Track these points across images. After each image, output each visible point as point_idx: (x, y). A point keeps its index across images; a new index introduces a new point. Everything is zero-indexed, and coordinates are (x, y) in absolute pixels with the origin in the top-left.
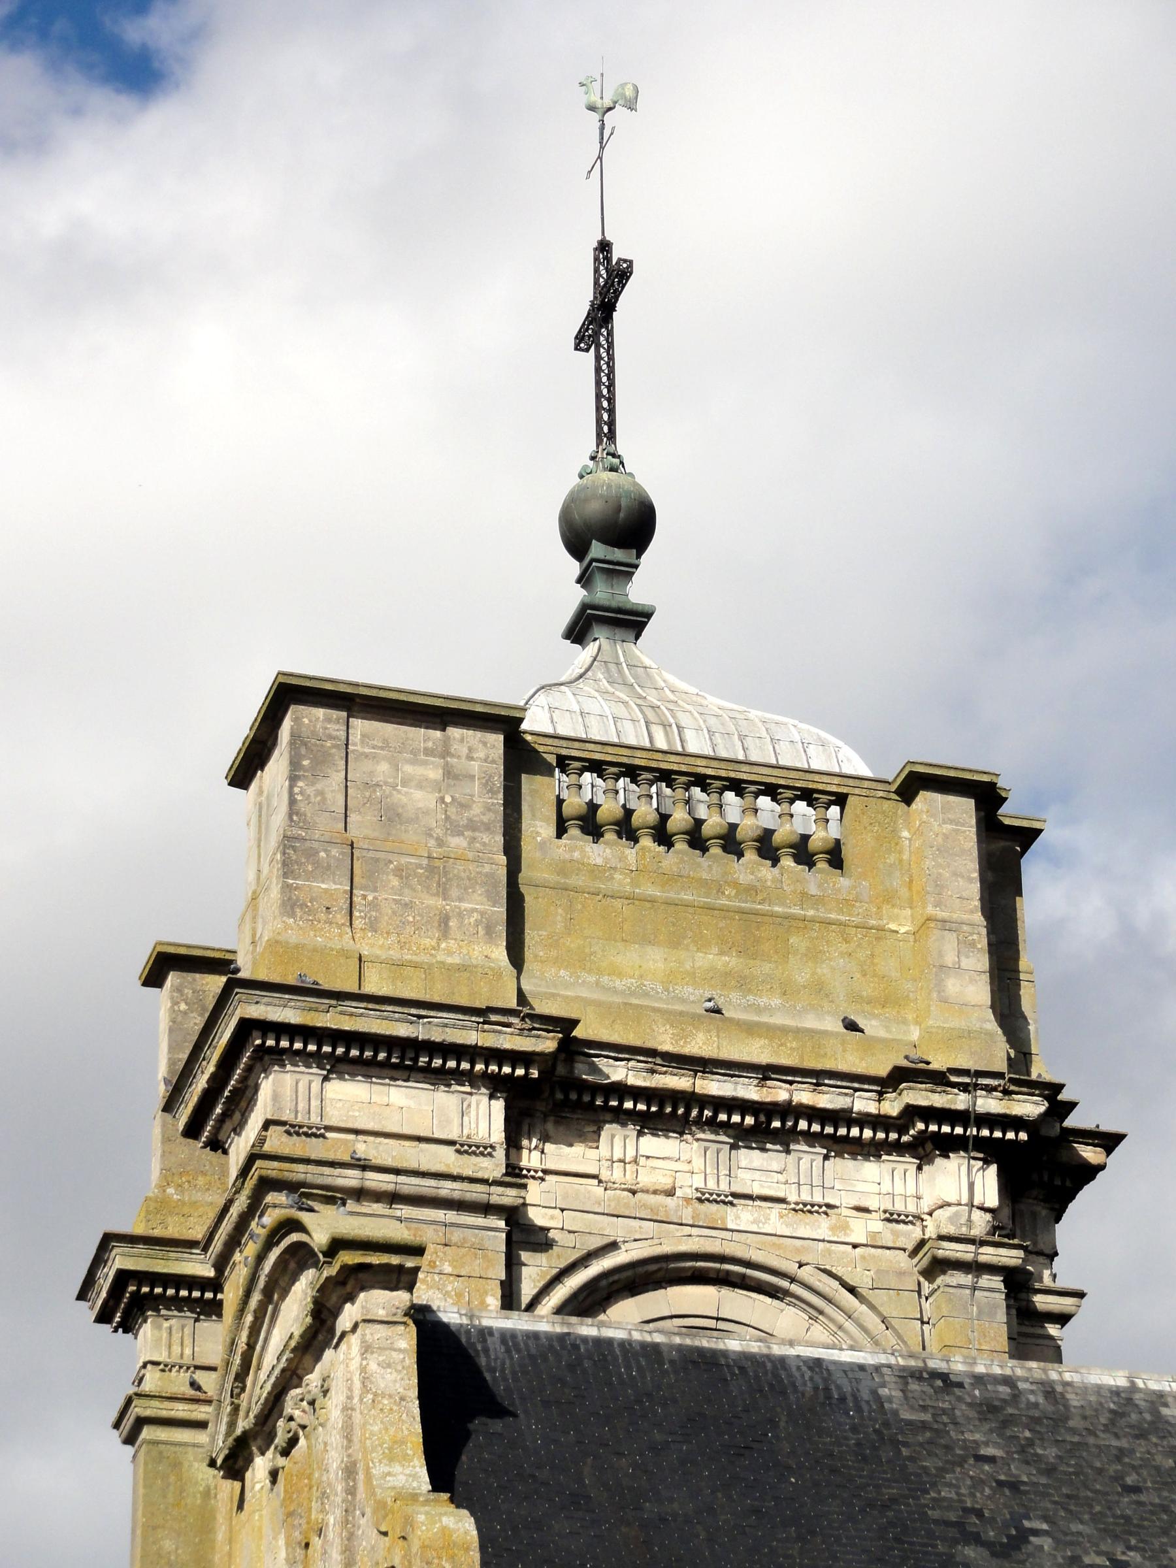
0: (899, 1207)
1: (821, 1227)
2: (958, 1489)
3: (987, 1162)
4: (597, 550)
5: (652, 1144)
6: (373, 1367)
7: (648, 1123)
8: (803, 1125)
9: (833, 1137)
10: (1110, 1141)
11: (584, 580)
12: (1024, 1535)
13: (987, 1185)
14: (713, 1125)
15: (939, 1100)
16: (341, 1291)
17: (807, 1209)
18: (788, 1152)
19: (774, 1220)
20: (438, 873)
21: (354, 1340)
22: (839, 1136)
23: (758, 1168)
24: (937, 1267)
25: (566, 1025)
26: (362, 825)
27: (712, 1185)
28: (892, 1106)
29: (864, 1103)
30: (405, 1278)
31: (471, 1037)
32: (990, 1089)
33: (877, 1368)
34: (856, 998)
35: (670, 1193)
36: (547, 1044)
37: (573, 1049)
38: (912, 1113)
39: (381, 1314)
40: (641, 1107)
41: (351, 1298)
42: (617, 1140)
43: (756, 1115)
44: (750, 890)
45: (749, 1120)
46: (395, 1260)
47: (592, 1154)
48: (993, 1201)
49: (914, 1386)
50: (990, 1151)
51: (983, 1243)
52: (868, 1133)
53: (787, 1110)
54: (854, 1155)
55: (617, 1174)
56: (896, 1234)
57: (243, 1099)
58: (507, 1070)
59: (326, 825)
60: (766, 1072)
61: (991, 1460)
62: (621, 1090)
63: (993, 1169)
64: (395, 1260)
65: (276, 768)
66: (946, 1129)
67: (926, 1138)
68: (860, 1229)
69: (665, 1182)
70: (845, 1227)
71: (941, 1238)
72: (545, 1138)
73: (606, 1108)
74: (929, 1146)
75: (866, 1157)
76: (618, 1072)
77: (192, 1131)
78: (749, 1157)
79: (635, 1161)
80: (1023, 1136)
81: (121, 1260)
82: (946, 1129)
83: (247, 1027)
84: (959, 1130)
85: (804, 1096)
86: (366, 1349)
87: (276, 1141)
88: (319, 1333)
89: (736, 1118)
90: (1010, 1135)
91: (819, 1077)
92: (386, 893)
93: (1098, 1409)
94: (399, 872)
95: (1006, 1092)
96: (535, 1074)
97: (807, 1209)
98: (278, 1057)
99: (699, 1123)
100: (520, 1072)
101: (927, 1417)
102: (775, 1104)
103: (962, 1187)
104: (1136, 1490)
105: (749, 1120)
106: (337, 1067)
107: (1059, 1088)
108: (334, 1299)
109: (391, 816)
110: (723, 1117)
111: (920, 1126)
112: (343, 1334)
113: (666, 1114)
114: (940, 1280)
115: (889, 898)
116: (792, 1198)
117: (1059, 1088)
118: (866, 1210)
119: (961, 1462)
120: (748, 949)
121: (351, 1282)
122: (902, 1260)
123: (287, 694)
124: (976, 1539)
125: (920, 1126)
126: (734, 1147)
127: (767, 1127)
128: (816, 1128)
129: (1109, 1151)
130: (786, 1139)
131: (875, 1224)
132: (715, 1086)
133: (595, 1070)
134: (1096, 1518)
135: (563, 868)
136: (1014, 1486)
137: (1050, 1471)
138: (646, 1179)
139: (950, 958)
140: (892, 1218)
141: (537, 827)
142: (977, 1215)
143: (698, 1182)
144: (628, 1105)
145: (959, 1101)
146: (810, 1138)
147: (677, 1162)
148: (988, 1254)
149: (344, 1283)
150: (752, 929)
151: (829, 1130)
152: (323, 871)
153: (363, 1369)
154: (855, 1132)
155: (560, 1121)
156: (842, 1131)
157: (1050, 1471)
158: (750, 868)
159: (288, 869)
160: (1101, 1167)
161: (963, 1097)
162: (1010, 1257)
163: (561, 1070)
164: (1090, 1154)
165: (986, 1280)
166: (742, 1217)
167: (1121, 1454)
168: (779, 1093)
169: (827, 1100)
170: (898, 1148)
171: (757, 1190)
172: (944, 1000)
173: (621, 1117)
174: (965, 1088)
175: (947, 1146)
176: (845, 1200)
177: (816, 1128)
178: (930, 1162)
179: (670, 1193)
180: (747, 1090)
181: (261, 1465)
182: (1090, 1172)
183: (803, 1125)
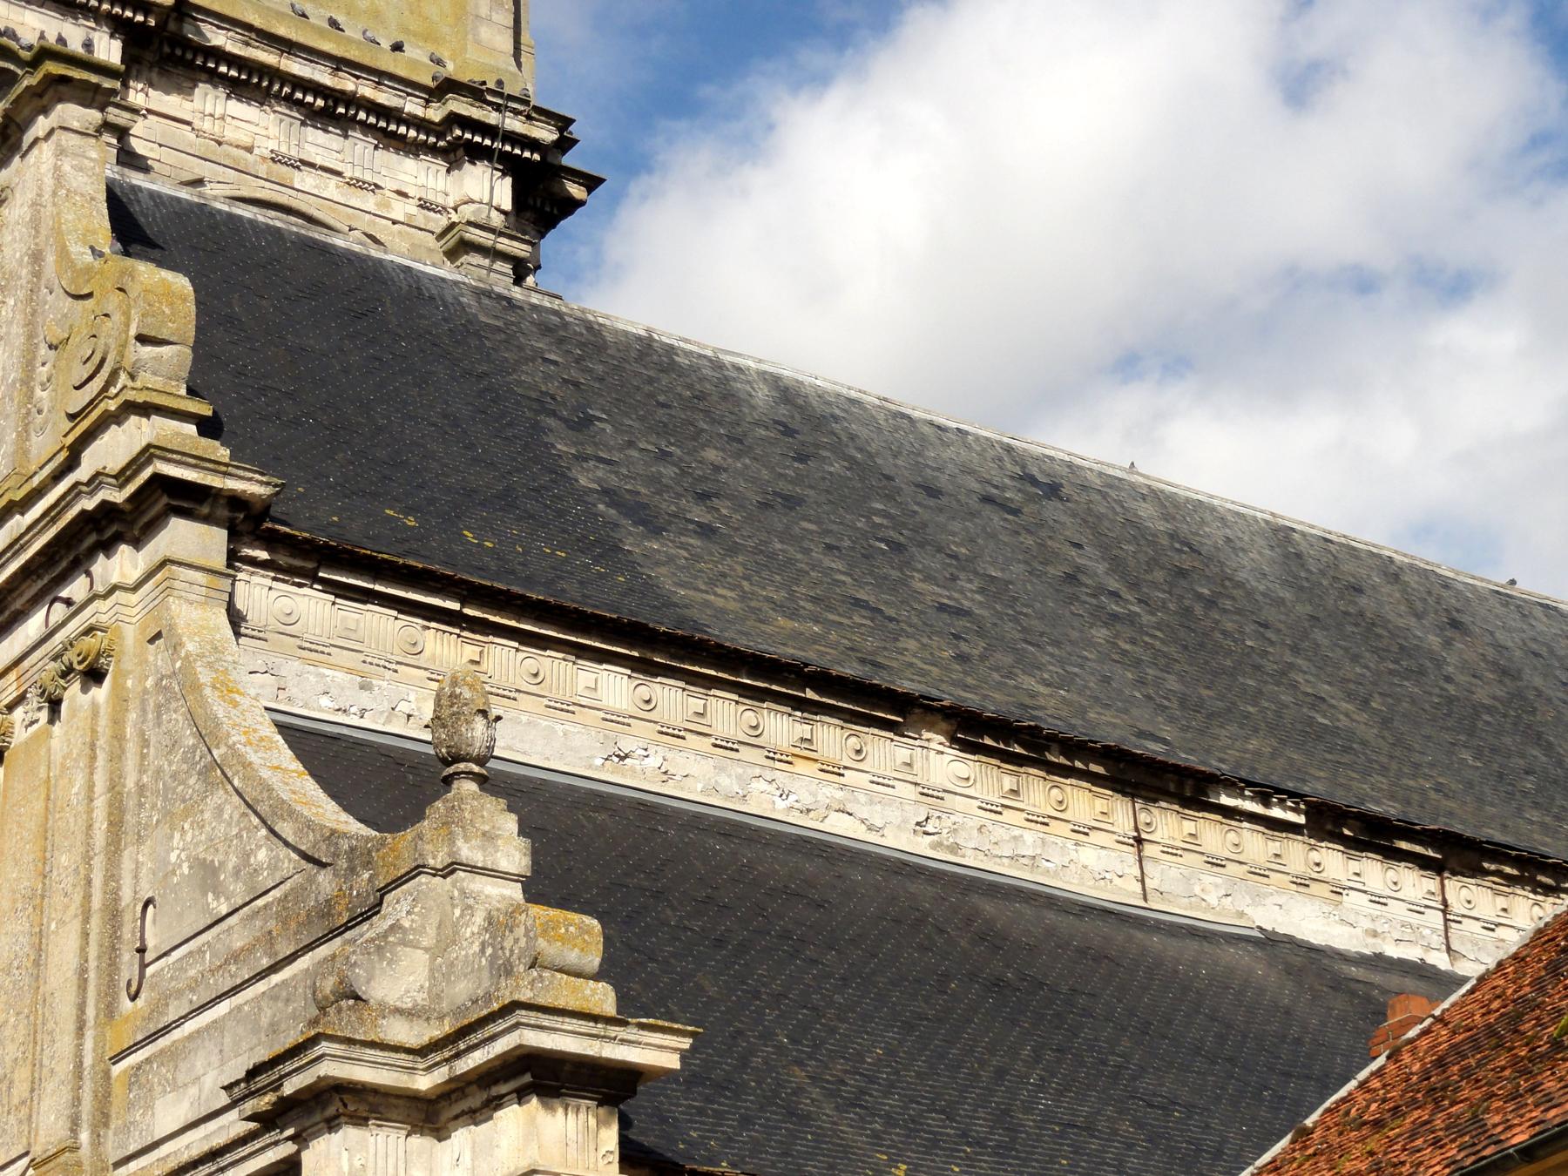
0: (431, 197)
1: (369, 202)
2: (531, 376)
3: (504, 174)
5: (236, 107)
6: (67, 168)
7: (237, 89)
8: (362, 115)
9: (383, 130)
10: (592, 183)
12: (589, 420)
13: (504, 193)
14: (289, 100)
16: (37, 103)
18: (346, 137)
19: (331, 188)
21: (45, 151)
22: (389, 129)
23: (320, 144)
24: (465, 246)
27: (284, 149)
28: (435, 114)
29: (413, 107)
30: (99, 98)
32: (516, 112)
33: (456, 283)
34: (406, 31)
35: (250, 150)
38: (454, 119)
39: (76, 125)
40: (233, 73)
41: (45, 111)
42: (207, 102)
43: (325, 98)
45: (320, 103)
46: (94, 79)
47: (187, 105)
48: (507, 205)
49: (486, 301)
50: (510, 166)
51: (501, 234)
52: (412, 133)
53: (351, 100)
54: (397, 151)
55: (207, 125)
56: (427, 219)
58: (129, 14)
60: (340, 64)
61: (555, 363)
62: (219, 54)
63: (508, 181)
64: (94, 79)
66: (478, 139)
67: (457, 145)
68: (400, 209)
69: (246, 140)
70: (388, 206)
71: (469, 223)
72: (151, 85)
73: (204, 68)
74: (461, 152)
75: (407, 154)
76: (218, 38)
78: (314, 135)
79: (222, 118)
80: (537, 157)
82: (478, 139)
84: (488, 142)
85: (366, 90)
86: (61, 152)
89: (309, 99)
90: (527, 154)
91: (381, 77)
93: (628, 347)
95: (529, 117)
96: (152, 22)
99: (277, 96)
100: (140, 18)
101: (500, 324)
102: (343, 92)
103: (485, 190)
104: (663, 405)
105: (320, 103)
107: (570, 121)
108: (26, 112)
110: (299, 95)
111: (458, 132)
112: (36, 141)
113: (252, 83)
114: (464, 259)
116: (348, 174)
117: (570, 121)
118: (405, 195)
119: (533, 360)
121: (58, 89)
122: (431, 238)
124: (553, 414)
125: (458, 132)
126: (303, 124)
127: (333, 111)
128: (372, 120)
129: (589, 192)
130: (345, 124)
131: (411, 208)
132: (296, 67)
133: (199, 33)
134: (642, 419)
136: (576, 384)
137: (601, 380)
138: (230, 134)
139: (484, 11)
140: (424, 205)
142: (494, 213)
143: (273, 145)
144: (223, 69)
145: (492, 118)
146: (366, 128)
147: (259, 127)
148: (504, 244)
149: (40, 96)
151: (382, 124)
153: (57, 168)
154: (402, 130)
155: (163, 72)
156: (393, 127)
157: (601, 380)
160: (581, 203)
161: (495, 114)
162: (520, 249)
163: (172, 26)
164: (576, 191)
165: (498, 265)
166: (306, 180)
167: (651, 381)
168: (347, 84)
169: (385, 97)
170: (433, 150)
171: (319, 161)
172: (478, 42)
173: (215, 78)
174: (497, 108)
175: (476, 153)
177: (372, 120)
178: (459, 167)
179: (250, 150)
182: (573, 205)
183: (362, 115)
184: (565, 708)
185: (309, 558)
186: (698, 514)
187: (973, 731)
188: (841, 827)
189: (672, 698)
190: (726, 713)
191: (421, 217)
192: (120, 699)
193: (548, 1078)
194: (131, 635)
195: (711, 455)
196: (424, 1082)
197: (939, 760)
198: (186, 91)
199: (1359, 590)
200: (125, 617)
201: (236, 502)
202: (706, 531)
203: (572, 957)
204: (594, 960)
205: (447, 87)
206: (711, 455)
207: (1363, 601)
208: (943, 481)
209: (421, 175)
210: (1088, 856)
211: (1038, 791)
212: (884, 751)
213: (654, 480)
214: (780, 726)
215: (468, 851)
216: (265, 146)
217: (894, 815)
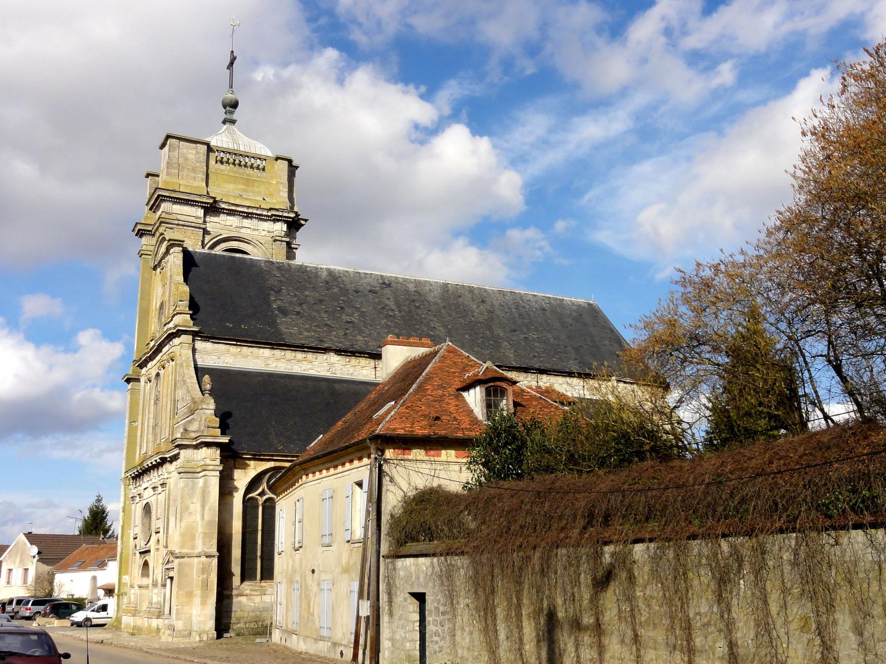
1: (257, 233)
2: (272, 281)
4: (228, 108)
5: (229, 218)
7: (228, 214)
10: (306, 220)
11: (226, 113)
13: (285, 227)
15: (277, 213)
17: (254, 230)
19: (249, 231)
20: (194, 170)
22: (260, 218)
23: (247, 222)
24: (275, 241)
25: (214, 198)
26: (181, 161)
28: (269, 214)
29: (265, 213)
31: (198, 199)
36: (211, 201)
37: (215, 201)
38: (273, 215)
42: (223, 217)
44: (248, 175)
50: (285, 222)
53: (251, 213)
57: (159, 207)
59: (175, 160)
60: (248, 207)
62: (224, 209)
65: (166, 148)
67: (276, 219)
68: (263, 233)
76: (223, 206)
77: (151, 209)
78: (245, 220)
81: (139, 227)
83: (159, 196)
85: (255, 211)
87: (164, 215)
88: (167, 253)
92: (185, 172)
94: (188, 169)
97: (254, 230)
98: (164, 200)
103: (280, 228)
106: (175, 203)
109: (186, 159)
113: (231, 213)
115: (272, 177)
120: (248, 185)
123: (168, 137)
127: (248, 216)
130: (251, 218)
131: (266, 233)
135: (216, 169)
141: (212, 162)
145: (281, 214)
147: (233, 221)
150: (248, 182)
152: (174, 168)
158: (249, 171)
159: (168, 168)
162: (288, 240)
164: (303, 222)
166: (243, 230)
168: (250, 211)
169: (258, 212)
173: (224, 213)
175: (278, 221)
176: (261, 229)
180: (245, 210)
181: (159, 270)
182: (303, 225)
184: (258, 357)
185: (207, 339)
186: (298, 309)
187: (339, 352)
188: (312, 373)
189: (278, 353)
190: (289, 354)
191: (268, 234)
192: (176, 364)
193: (208, 445)
194: (178, 354)
195: (307, 293)
196: (194, 443)
197: (333, 358)
198: (219, 216)
199: (460, 297)
200: (177, 350)
201: (193, 331)
202: (298, 313)
203: (214, 425)
204: (218, 425)
205: (271, 209)
206: (307, 293)
207: (460, 299)
208: (361, 288)
209: (267, 225)
210: (364, 372)
211: (354, 361)
212: (322, 357)
213: (291, 302)
214: (300, 355)
215: (204, 407)
216: (235, 225)
217: (323, 369)
